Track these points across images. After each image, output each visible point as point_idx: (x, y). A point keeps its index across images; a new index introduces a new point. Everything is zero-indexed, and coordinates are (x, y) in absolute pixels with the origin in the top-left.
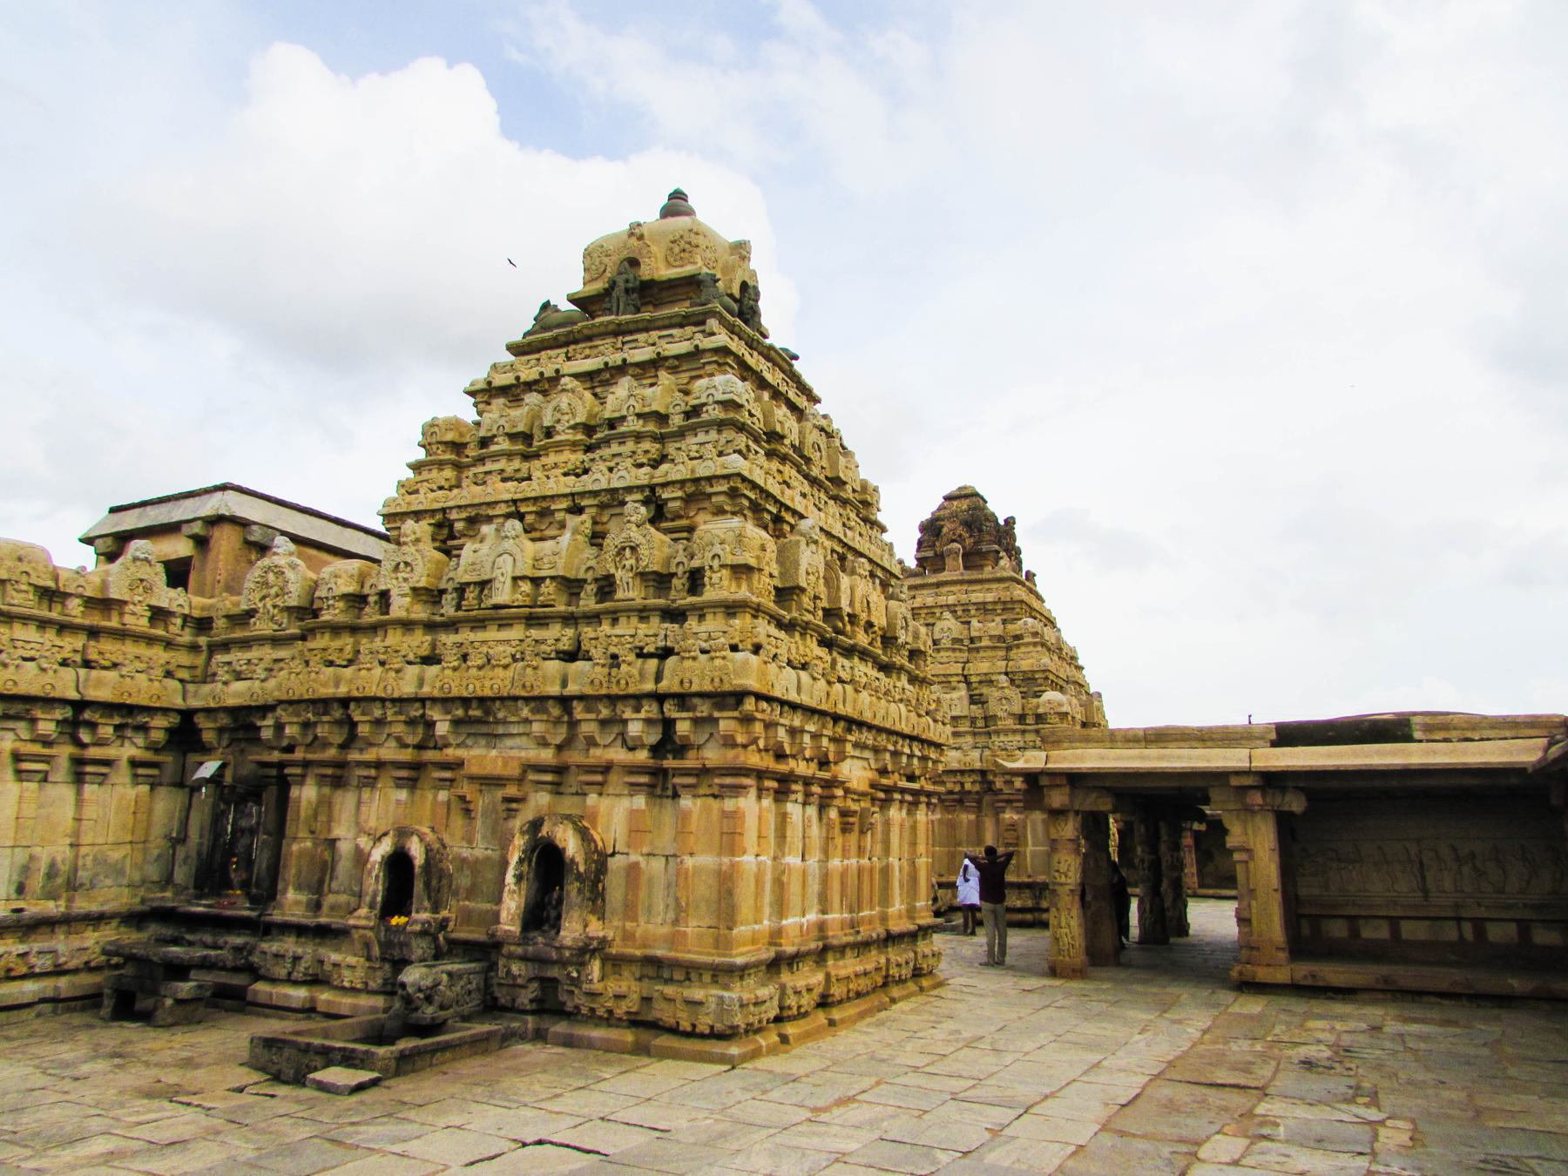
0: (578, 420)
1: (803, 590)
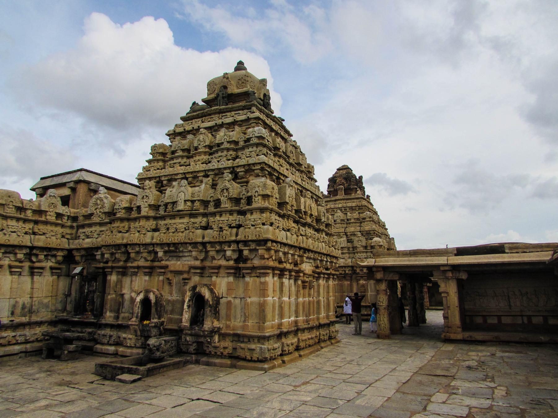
1: (288, 203)
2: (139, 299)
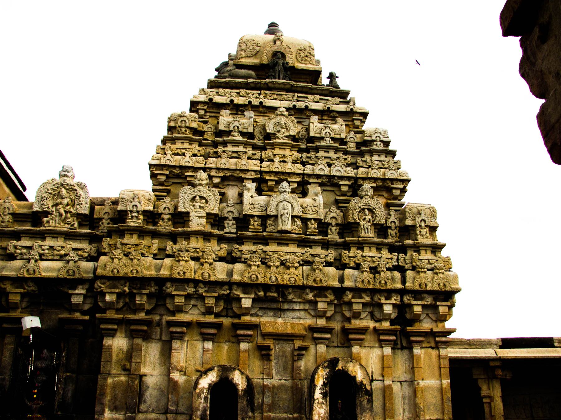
0: (291, 133)
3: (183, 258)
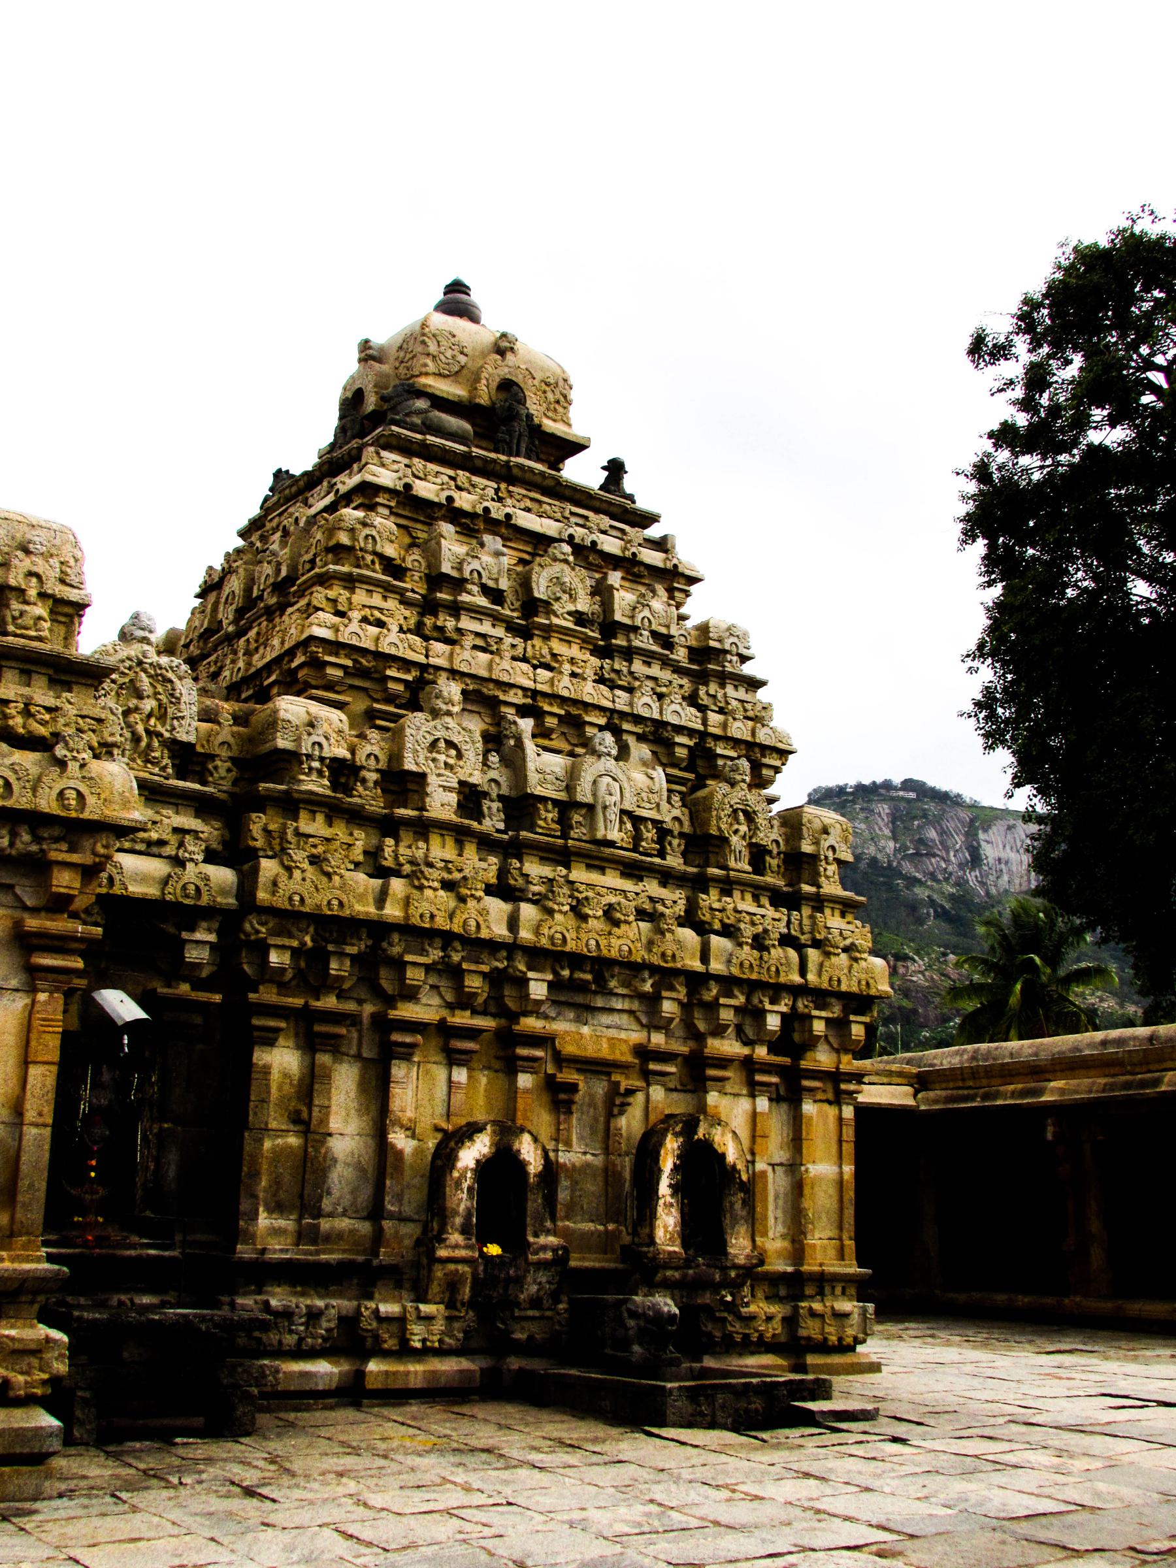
0: (580, 608)
2: (470, 1155)
3: (431, 884)
